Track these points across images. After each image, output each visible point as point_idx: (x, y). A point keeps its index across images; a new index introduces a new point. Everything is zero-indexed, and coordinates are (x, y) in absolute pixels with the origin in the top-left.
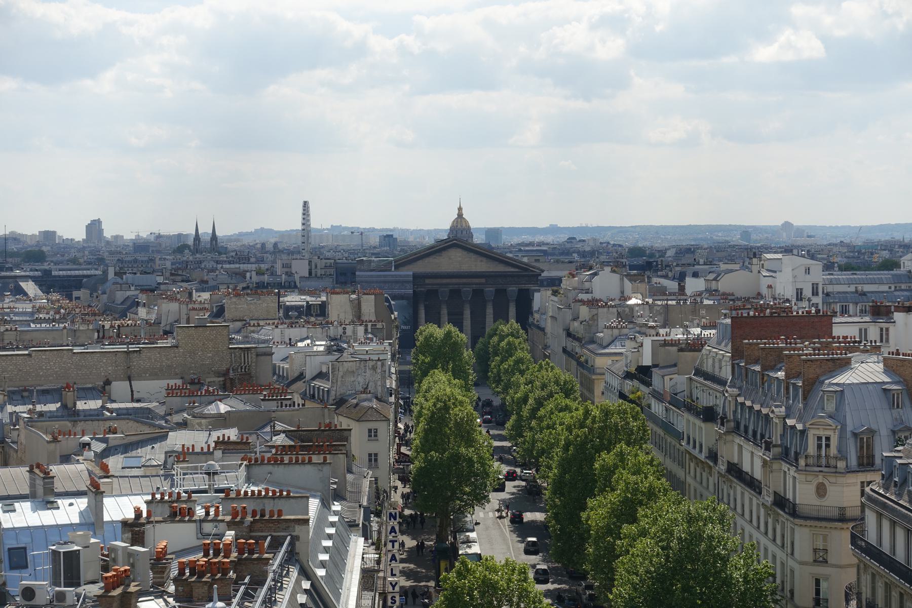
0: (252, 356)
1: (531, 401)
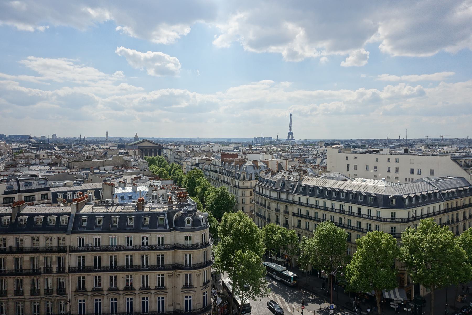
0: (128, 162)
1: (173, 170)
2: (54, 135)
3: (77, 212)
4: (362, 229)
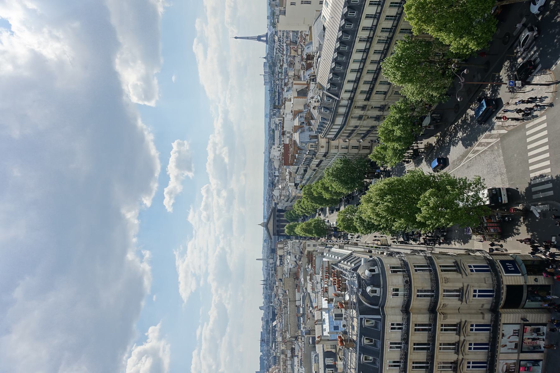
0: (291, 273)
4: (397, 14)
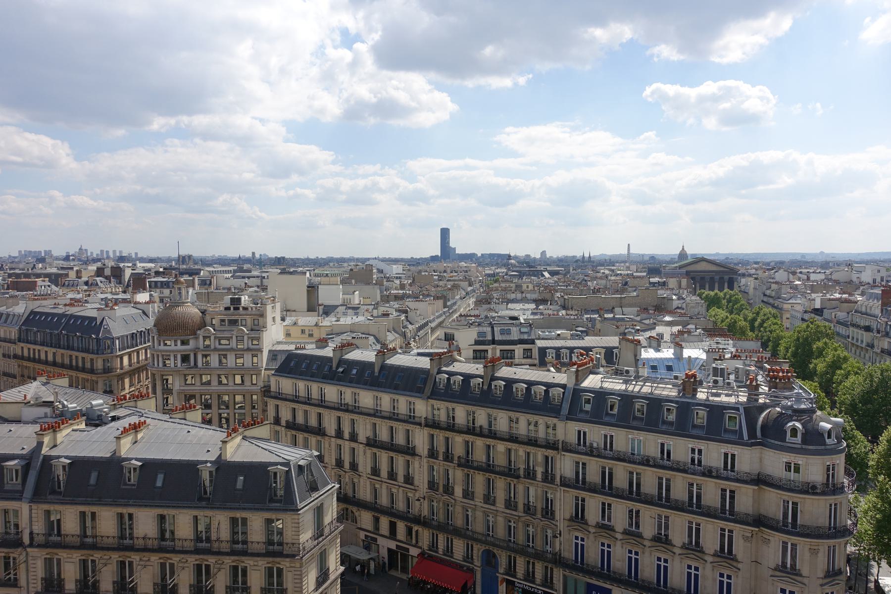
0: (666, 300)
1: (759, 320)
2: (543, 253)
3: (576, 385)
